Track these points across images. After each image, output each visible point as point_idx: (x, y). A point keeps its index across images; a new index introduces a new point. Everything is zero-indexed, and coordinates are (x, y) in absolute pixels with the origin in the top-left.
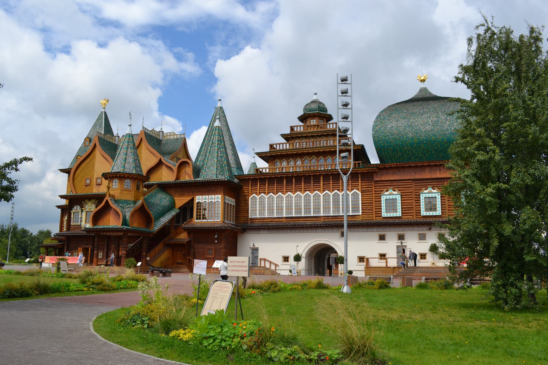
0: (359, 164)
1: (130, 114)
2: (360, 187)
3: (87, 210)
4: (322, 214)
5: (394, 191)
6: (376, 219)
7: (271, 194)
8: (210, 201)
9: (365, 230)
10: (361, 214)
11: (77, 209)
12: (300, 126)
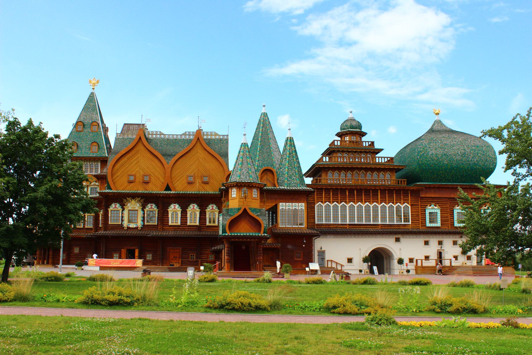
0: (404, 181)
2: (410, 201)
3: (130, 208)
4: (380, 223)
5: (435, 206)
6: (422, 229)
8: (293, 208)
9: (415, 236)
10: (410, 223)
11: (115, 207)
12: (337, 141)
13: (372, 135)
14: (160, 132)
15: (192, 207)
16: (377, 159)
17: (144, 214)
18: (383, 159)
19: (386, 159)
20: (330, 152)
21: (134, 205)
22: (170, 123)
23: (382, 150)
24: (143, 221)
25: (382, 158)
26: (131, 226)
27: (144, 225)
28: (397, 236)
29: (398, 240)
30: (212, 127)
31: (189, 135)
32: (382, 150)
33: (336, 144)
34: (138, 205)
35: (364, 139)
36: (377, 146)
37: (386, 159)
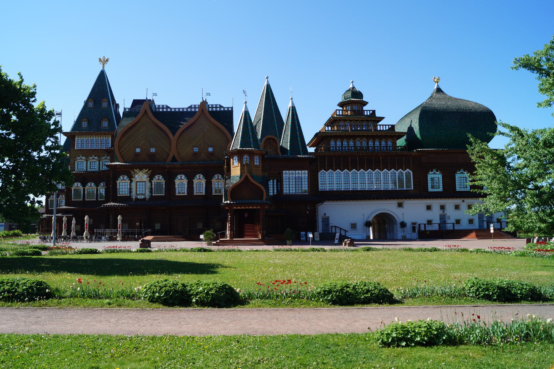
1: (244, 92)
3: (138, 180)
12: (339, 110)
13: (374, 103)
14: (167, 106)
15: (198, 177)
16: (379, 127)
17: (152, 185)
18: (384, 126)
19: (387, 127)
20: (332, 122)
21: (141, 176)
22: (176, 97)
23: (383, 118)
24: (151, 192)
25: (383, 125)
26: (139, 197)
27: (152, 196)
28: (400, 201)
29: (400, 205)
30: (218, 99)
31: (195, 108)
32: (383, 118)
33: (338, 114)
34: (146, 176)
35: (365, 108)
36: (378, 115)
37: (387, 127)
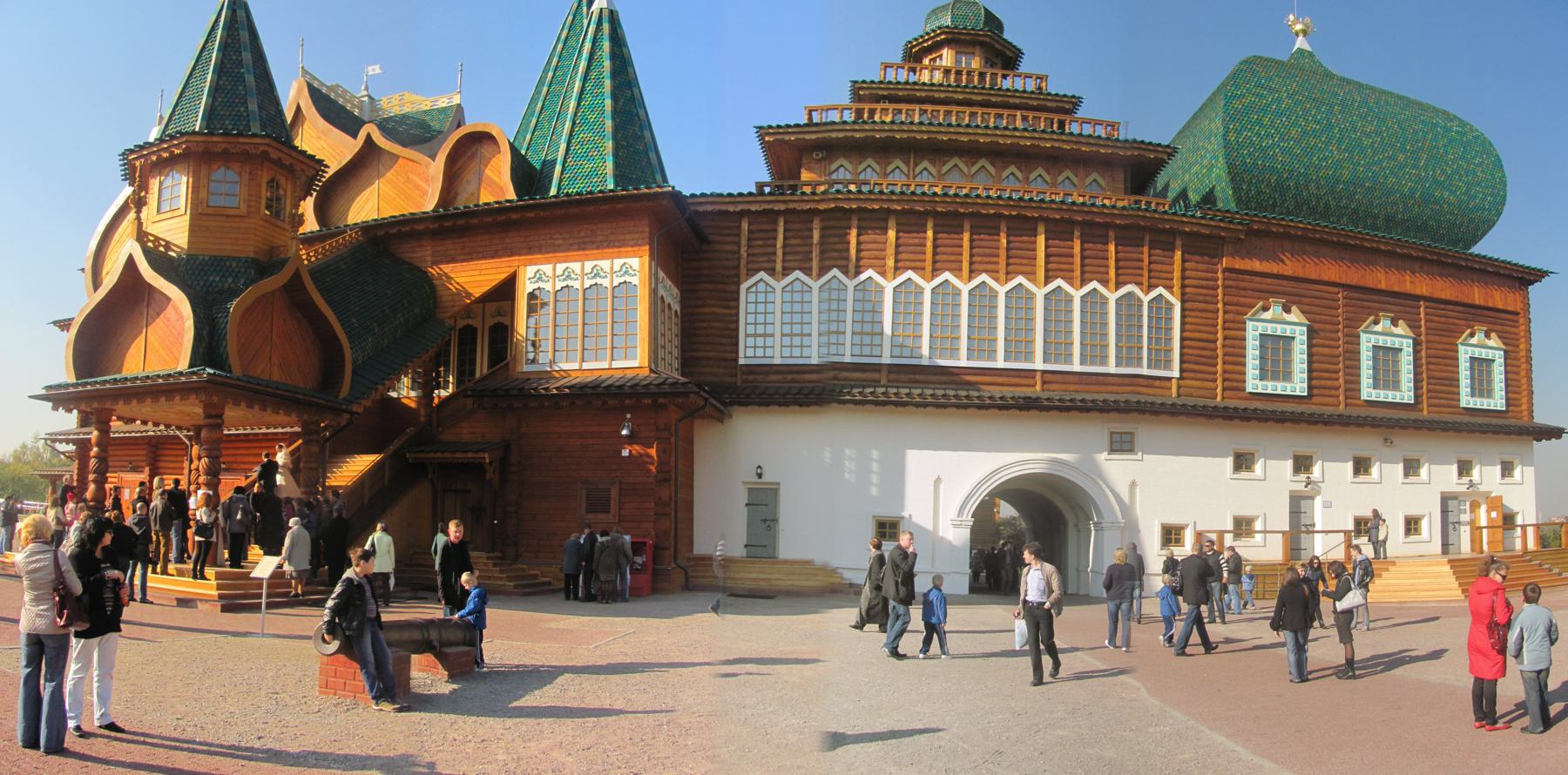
4: (1039, 364)
7: (835, 272)
10: (1176, 374)
